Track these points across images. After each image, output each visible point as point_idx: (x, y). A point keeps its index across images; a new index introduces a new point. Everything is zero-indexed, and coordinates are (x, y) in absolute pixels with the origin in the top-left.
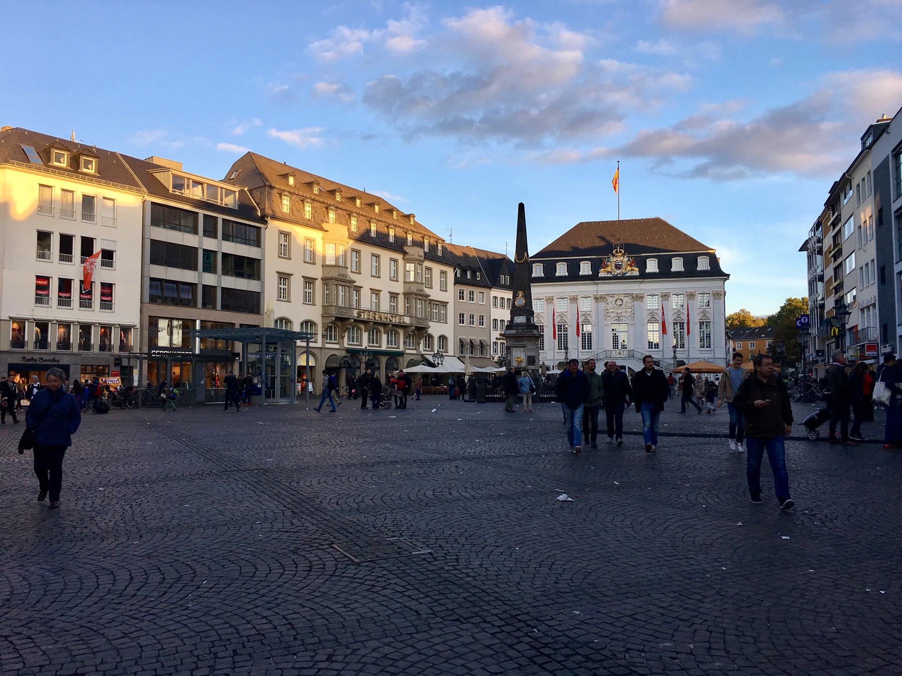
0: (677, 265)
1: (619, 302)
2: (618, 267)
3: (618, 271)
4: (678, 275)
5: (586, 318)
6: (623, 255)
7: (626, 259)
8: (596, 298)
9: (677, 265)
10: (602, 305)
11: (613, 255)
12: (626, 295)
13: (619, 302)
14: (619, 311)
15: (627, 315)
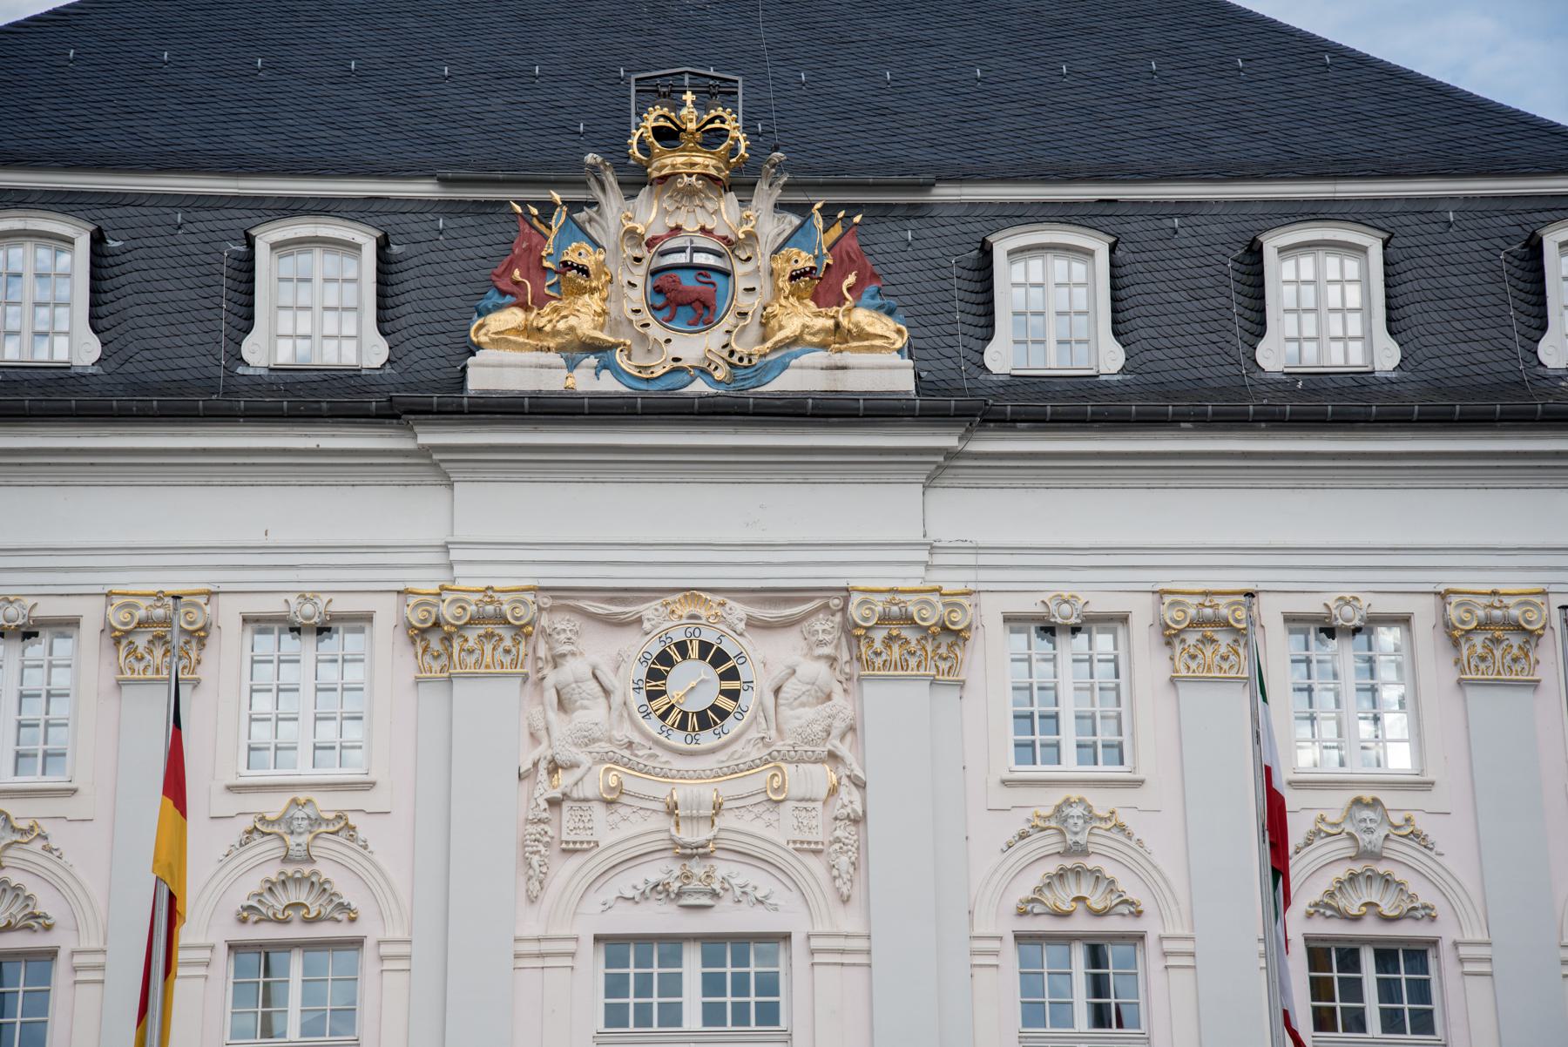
0: (1325, 305)
1: (693, 684)
2: (684, 296)
3: (692, 347)
4: (1329, 405)
5: (297, 871)
6: (740, 182)
7: (771, 226)
8: (429, 634)
9: (1325, 305)
10: (492, 707)
11: (635, 181)
12: (779, 605)
13: (693, 684)
14: (694, 792)
15: (778, 830)
